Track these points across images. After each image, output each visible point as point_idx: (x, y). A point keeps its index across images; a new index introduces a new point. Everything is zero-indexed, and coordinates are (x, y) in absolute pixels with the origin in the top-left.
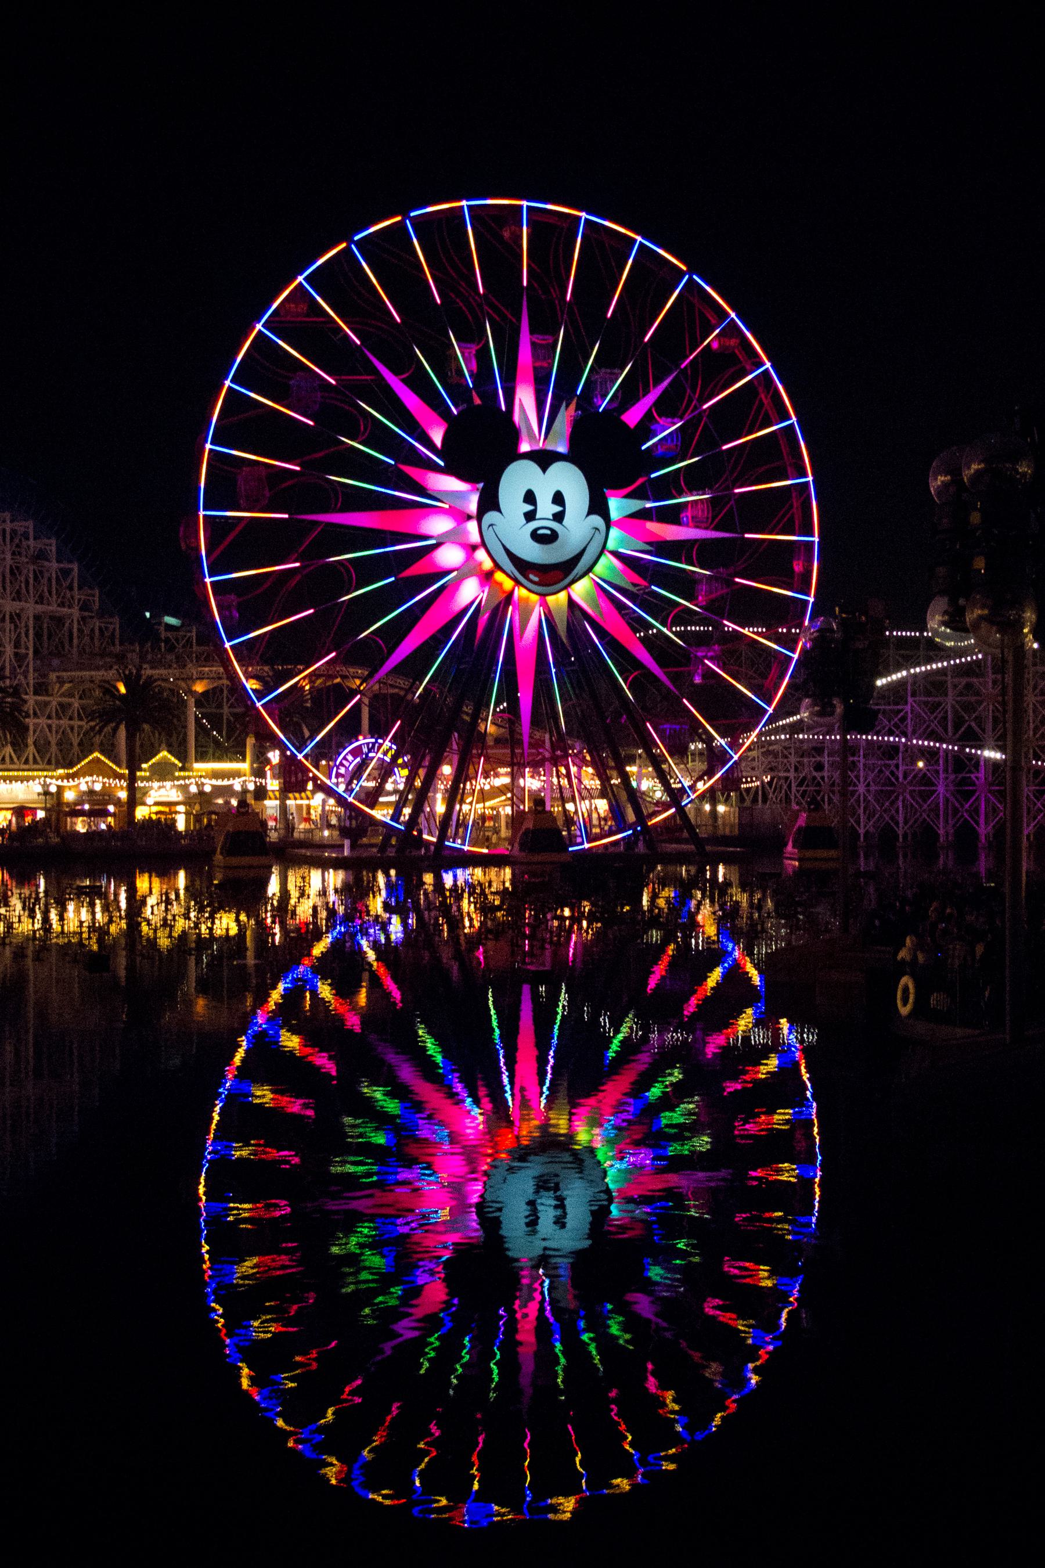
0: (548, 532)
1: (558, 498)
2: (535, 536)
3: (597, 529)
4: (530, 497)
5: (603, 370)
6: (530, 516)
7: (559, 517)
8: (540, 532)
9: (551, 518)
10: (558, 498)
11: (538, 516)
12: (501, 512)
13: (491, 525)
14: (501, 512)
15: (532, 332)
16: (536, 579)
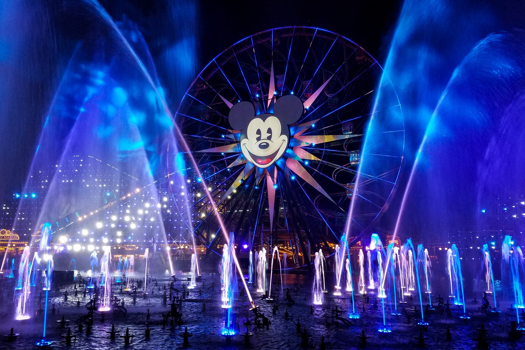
0: (265, 144)
1: (269, 131)
2: (261, 146)
3: (284, 140)
4: (259, 132)
5: (304, 82)
6: (259, 139)
7: (269, 138)
8: (262, 144)
9: (267, 139)
10: (269, 131)
11: (261, 139)
12: (248, 139)
13: (244, 144)
14: (248, 139)
15: (275, 75)
16: (260, 161)
